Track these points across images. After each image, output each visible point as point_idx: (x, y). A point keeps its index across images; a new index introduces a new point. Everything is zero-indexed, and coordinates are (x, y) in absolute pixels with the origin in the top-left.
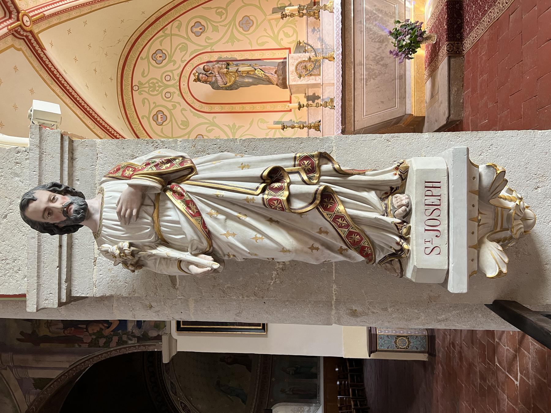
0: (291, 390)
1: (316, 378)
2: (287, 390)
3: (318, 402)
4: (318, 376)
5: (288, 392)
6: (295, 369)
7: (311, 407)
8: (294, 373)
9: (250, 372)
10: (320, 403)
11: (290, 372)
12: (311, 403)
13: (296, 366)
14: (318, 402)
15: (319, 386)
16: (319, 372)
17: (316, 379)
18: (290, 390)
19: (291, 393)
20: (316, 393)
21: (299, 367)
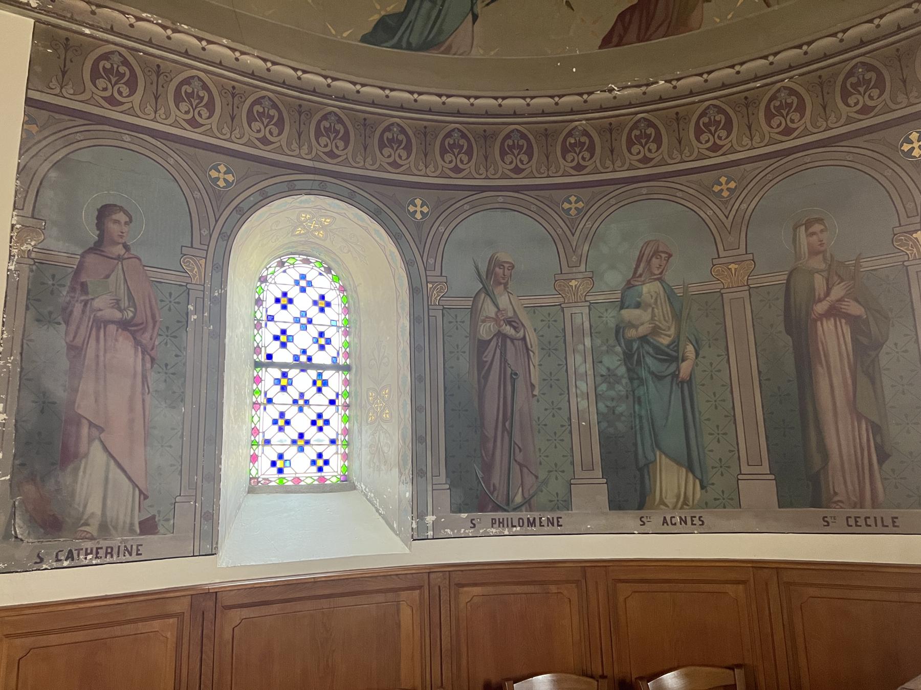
0: (508, 330)
1: (617, 504)
2: (503, 301)
3: (430, 519)
4: (629, 519)
5: (489, 309)
6: (665, 341)
7: (395, 471)
8: (632, 333)
9: (606, 42)
10: (419, 536)
11: (638, 306)
12: (418, 473)
13: (690, 348)
14: (430, 519)
15: (555, 526)
16: (668, 526)
17: (603, 499)
18: (509, 322)
19: (485, 331)
20: (497, 508)
21: (685, 368)
